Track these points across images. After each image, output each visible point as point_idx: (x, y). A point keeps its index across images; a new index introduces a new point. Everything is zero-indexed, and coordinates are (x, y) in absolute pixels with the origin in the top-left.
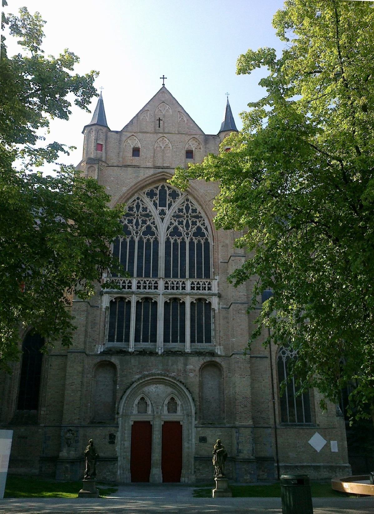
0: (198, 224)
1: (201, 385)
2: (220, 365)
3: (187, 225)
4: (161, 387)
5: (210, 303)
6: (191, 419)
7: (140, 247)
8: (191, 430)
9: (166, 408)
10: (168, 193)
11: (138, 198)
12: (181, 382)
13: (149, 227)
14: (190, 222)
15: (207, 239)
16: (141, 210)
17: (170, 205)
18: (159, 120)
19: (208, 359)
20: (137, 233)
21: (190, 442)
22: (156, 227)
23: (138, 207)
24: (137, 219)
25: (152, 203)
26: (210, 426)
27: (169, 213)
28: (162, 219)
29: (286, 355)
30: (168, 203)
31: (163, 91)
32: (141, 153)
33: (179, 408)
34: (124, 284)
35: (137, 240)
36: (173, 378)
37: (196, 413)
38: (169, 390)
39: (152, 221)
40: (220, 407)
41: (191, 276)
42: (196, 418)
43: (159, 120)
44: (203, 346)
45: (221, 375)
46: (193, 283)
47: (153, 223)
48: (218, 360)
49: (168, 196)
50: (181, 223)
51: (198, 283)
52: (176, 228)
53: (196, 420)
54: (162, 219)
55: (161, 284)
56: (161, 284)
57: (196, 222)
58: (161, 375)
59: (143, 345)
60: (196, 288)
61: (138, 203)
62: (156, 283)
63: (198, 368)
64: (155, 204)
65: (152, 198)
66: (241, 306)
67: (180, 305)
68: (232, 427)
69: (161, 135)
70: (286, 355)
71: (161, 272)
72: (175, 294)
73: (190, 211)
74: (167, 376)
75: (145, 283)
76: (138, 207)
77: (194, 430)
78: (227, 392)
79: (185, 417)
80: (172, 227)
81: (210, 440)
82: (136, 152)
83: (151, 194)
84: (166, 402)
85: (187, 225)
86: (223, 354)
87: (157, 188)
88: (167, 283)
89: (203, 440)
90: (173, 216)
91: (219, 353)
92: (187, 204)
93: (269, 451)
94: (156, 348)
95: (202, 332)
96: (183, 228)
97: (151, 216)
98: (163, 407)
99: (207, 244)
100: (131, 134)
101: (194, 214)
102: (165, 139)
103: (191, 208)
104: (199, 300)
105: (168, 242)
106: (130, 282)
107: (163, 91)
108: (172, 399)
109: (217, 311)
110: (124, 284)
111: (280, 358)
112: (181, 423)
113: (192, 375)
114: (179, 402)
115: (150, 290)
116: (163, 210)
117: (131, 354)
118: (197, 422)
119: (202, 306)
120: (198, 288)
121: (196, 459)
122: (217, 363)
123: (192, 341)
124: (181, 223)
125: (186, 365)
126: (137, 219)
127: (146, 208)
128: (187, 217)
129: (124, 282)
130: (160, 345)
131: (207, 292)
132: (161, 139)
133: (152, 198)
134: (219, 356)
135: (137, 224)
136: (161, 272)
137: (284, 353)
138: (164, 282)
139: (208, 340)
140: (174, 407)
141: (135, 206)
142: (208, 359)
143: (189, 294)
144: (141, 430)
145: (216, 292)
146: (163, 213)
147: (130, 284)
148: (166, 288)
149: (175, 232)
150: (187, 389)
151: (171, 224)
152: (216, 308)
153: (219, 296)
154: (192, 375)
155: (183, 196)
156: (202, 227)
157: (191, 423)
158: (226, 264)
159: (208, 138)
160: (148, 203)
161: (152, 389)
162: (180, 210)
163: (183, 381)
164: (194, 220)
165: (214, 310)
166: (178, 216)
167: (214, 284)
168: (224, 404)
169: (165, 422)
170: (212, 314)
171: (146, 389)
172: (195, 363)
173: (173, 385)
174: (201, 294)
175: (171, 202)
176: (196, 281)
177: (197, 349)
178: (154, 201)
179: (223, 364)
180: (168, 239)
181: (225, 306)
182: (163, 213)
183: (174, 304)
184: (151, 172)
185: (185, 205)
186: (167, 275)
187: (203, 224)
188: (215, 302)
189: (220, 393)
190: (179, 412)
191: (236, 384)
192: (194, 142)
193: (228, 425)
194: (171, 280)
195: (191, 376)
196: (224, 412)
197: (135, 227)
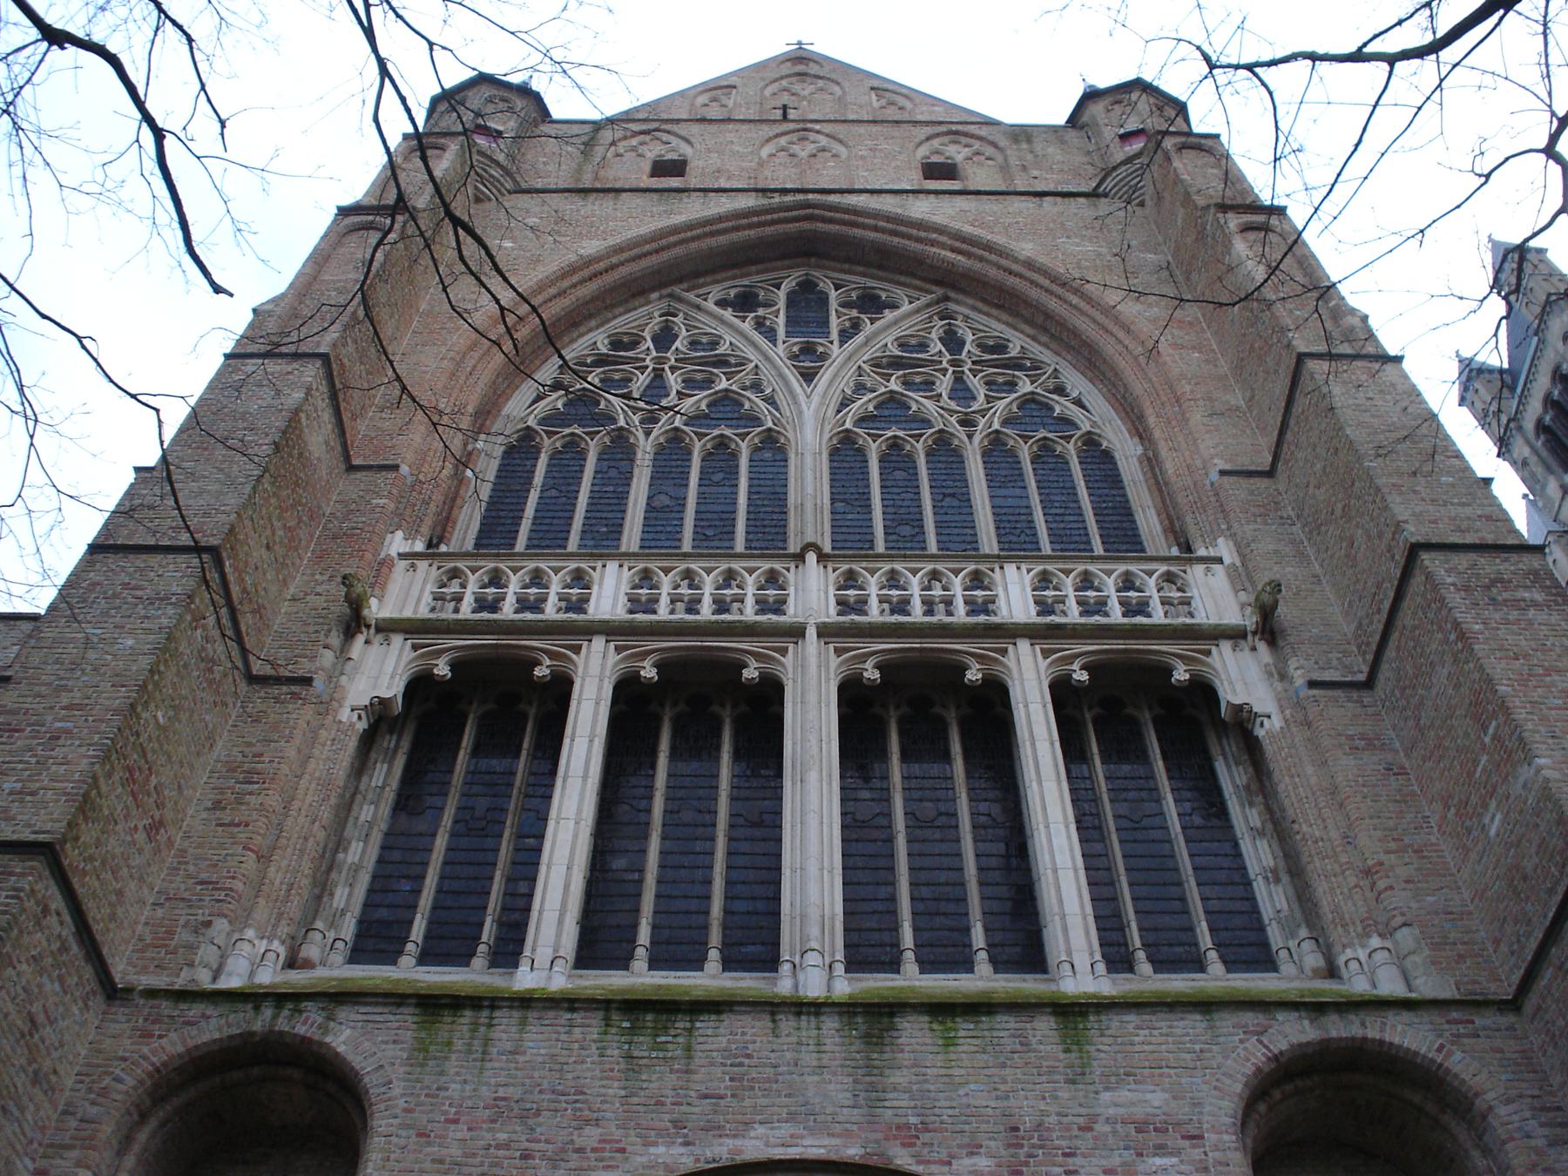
5: (1203, 691)
24: (658, 374)
47: (756, 386)
62: (772, 578)
88: (850, 579)
90: (876, 363)
97: (743, 362)
99: (1097, 455)
102: (812, 136)
103: (969, 337)
105: (845, 451)
109: (1271, 725)
141: (647, 334)
151: (860, 388)
153: (1268, 629)
158: (1262, 483)
165: (1242, 725)
180: (847, 438)
188: (1241, 678)
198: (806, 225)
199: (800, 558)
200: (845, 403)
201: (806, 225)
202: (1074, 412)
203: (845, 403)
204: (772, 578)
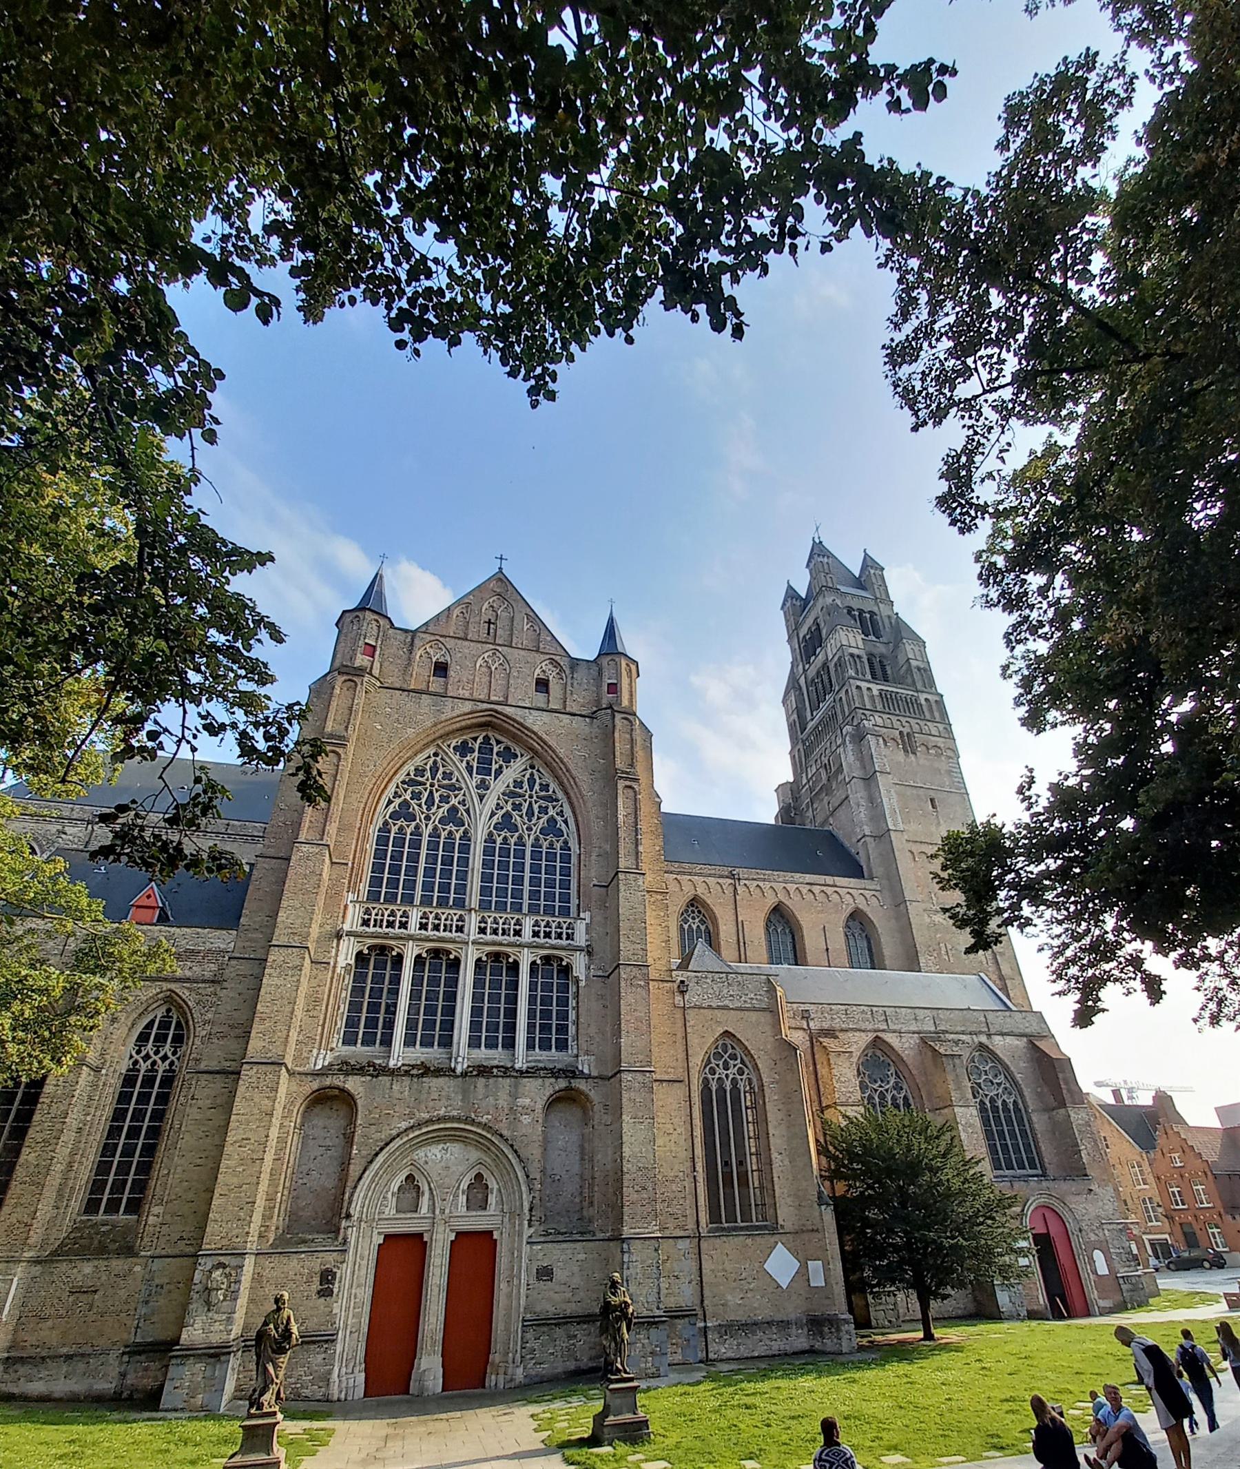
0: (551, 812)
1: (546, 1143)
2: (587, 1096)
3: (530, 813)
4: (455, 1149)
6: (521, 1225)
7: (433, 846)
8: (520, 1251)
9: (462, 1199)
10: (496, 750)
11: (436, 754)
12: (501, 1136)
13: (454, 810)
14: (536, 807)
15: (566, 842)
16: (439, 775)
17: (499, 772)
18: (489, 622)
19: (562, 1083)
20: (428, 818)
21: (516, 1281)
22: (468, 811)
23: (434, 769)
24: (431, 792)
25: (464, 764)
26: (561, 1238)
27: (498, 787)
28: (481, 797)
29: (717, 1076)
30: (494, 767)
31: (500, 578)
32: (451, 673)
33: (492, 1199)
34: (391, 919)
35: (426, 832)
36: (485, 1126)
37: (531, 1210)
38: (474, 1155)
39: (460, 798)
40: (581, 1193)
41: (533, 910)
42: (530, 1221)
43: (489, 622)
44: (553, 1057)
45: (586, 1119)
46: (536, 924)
47: (463, 803)
48: (581, 1085)
49: (495, 756)
50: (517, 807)
51: (548, 925)
52: (507, 816)
53: (530, 1226)
54: (481, 797)
55: (473, 922)
56: (473, 922)
57: (547, 807)
58: (459, 1120)
59: (418, 1054)
60: (542, 934)
61: (435, 762)
62: (461, 919)
63: (539, 1106)
64: (469, 768)
65: (463, 755)
66: (635, 971)
67: (508, 968)
68: (609, 1240)
69: (492, 647)
70: (717, 1076)
71: (474, 899)
72: (501, 944)
73: (537, 787)
74: (473, 1122)
75: (437, 917)
76: (434, 769)
77: (526, 1249)
78: (599, 1156)
79: (506, 1220)
80: (501, 813)
81: (559, 1274)
82: (441, 669)
83: (463, 749)
84: (464, 1185)
85: (530, 813)
86: (595, 1074)
87: (475, 739)
88: (483, 921)
89: (545, 1273)
91: (586, 1071)
92: (532, 774)
93: (685, 1296)
94: (450, 1059)
95: (551, 1030)
96: (521, 816)
98: (456, 1196)
100: (433, 638)
101: (543, 793)
104: (547, 959)
105: (490, 839)
106: (405, 914)
107: (500, 578)
108: (479, 1176)
109: (582, 984)
110: (391, 919)
111: (706, 1082)
112: (496, 1235)
113: (526, 1119)
114: (493, 1184)
115: (447, 934)
116: (483, 781)
117: (393, 1073)
118: (532, 1230)
119: (554, 969)
120: (547, 935)
121: (527, 1325)
122: (582, 1093)
123: (530, 1046)
124: (517, 807)
125: (514, 1096)
126: (431, 792)
127: (451, 774)
128: (531, 797)
129: (392, 914)
130: (464, 1055)
131: (564, 942)
132: (490, 653)
133: (463, 755)
134: (588, 1077)
135: (430, 802)
136: (474, 899)
137: (713, 1072)
138: (479, 918)
139: (562, 1045)
140: (480, 1196)
142: (562, 1083)
143: (529, 946)
144: (403, 1254)
145: (583, 944)
146: (483, 785)
147: (404, 919)
148: (482, 931)
149: (506, 823)
150: (516, 1152)
152: (582, 977)
153: (589, 951)
154: (526, 1119)
155: (524, 759)
156: (559, 818)
157: (520, 1235)
159: (575, 663)
160: (458, 765)
161: (435, 1152)
162: (518, 784)
163: (505, 1133)
164: (543, 803)
165: (577, 981)
166: (512, 794)
167: (580, 927)
168: (591, 1186)
169: (459, 1234)
170: (572, 989)
171: (420, 1154)
172: (536, 1093)
173: (482, 1144)
174: (554, 947)
175: (501, 767)
176: (544, 919)
177: (539, 1061)
178: (468, 763)
179: (592, 1094)
180: (491, 834)
181: (600, 973)
182: (483, 785)
183: (499, 966)
184: (468, 707)
185: (528, 776)
186: (484, 906)
187: (561, 814)
189: (582, 1159)
190: (493, 1207)
191: (625, 1139)
192: (550, 666)
193: (600, 1236)
194: (490, 916)
195: (525, 1122)
196: (591, 1204)
197: (425, 807)
198: (489, 719)
199: (470, 910)
200: (493, 814)
201: (489, 719)
202: (563, 827)
203: (493, 814)
204: (461, 919)
